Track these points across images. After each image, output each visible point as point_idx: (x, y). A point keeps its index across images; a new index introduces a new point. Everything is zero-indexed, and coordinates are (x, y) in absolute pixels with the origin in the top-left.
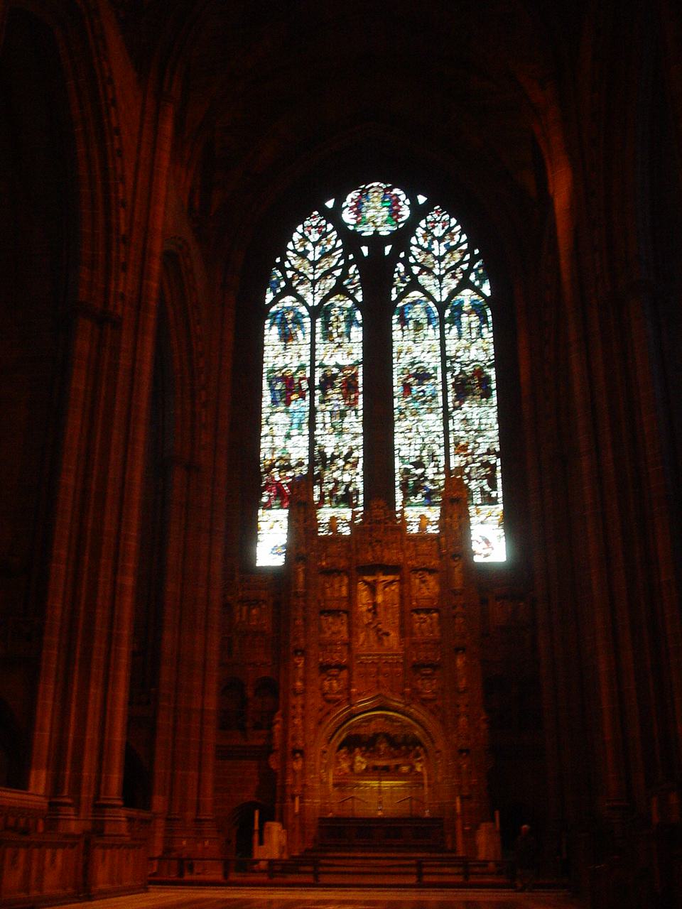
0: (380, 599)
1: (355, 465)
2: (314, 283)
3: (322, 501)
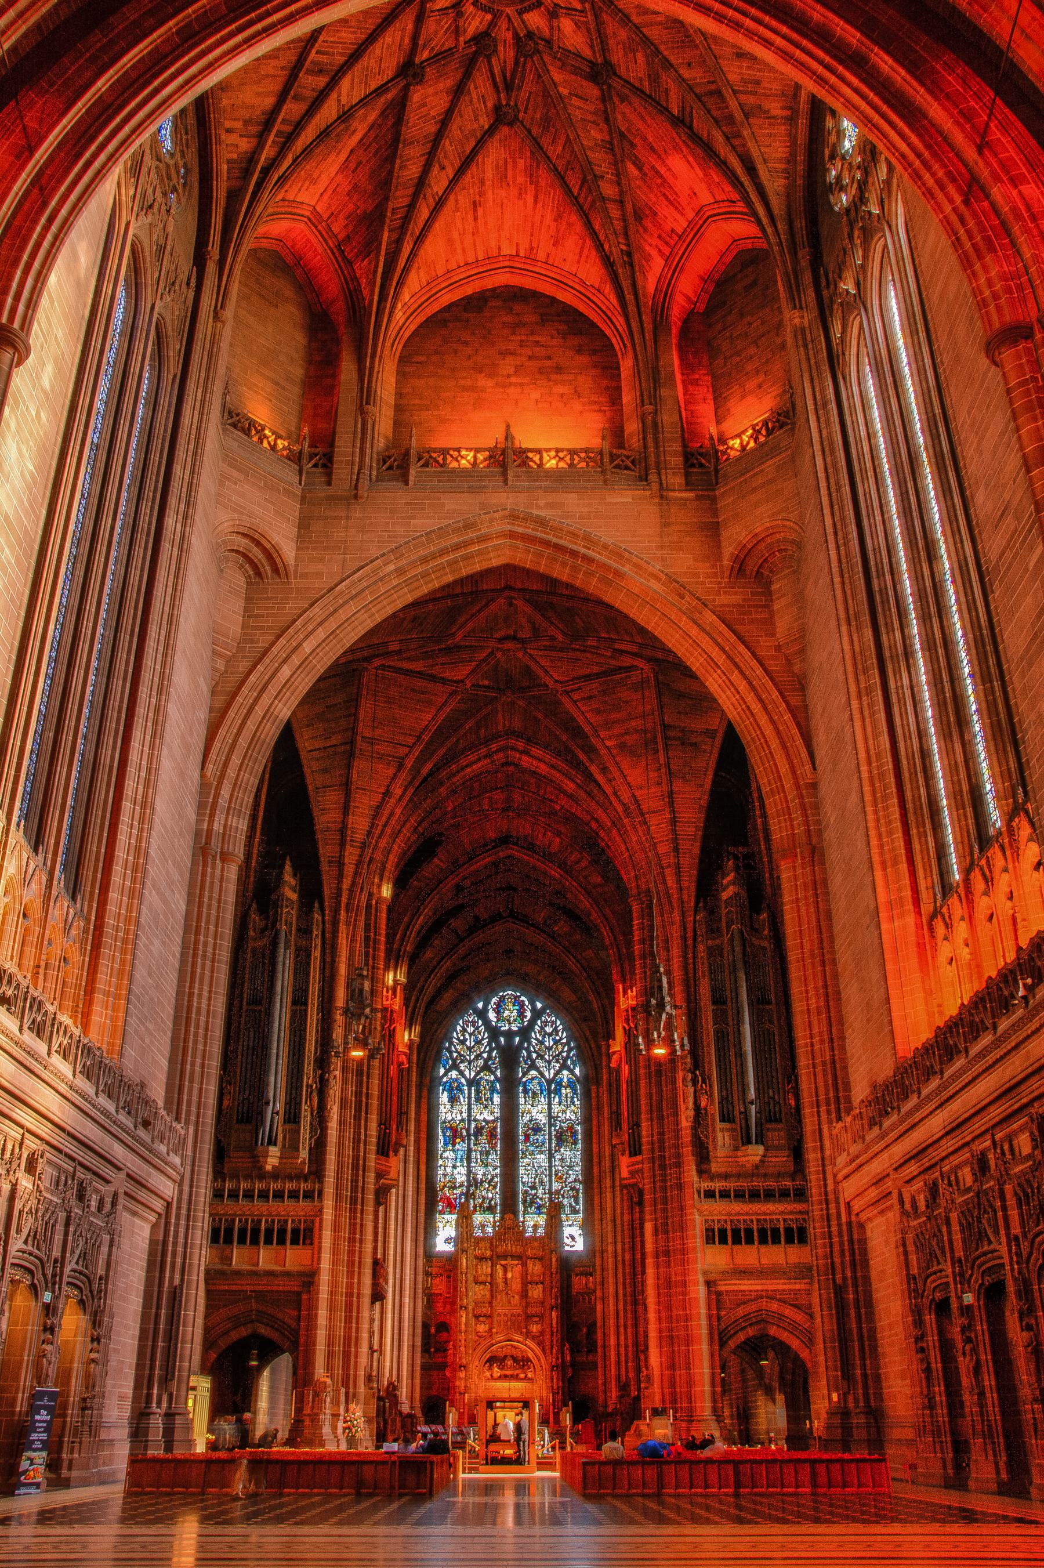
0: (509, 1275)
1: (495, 1187)
2: (470, 1062)
3: (475, 1210)
